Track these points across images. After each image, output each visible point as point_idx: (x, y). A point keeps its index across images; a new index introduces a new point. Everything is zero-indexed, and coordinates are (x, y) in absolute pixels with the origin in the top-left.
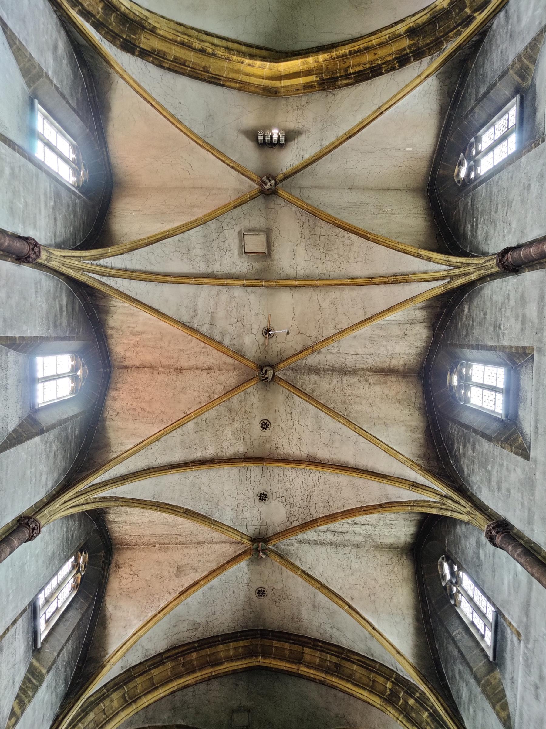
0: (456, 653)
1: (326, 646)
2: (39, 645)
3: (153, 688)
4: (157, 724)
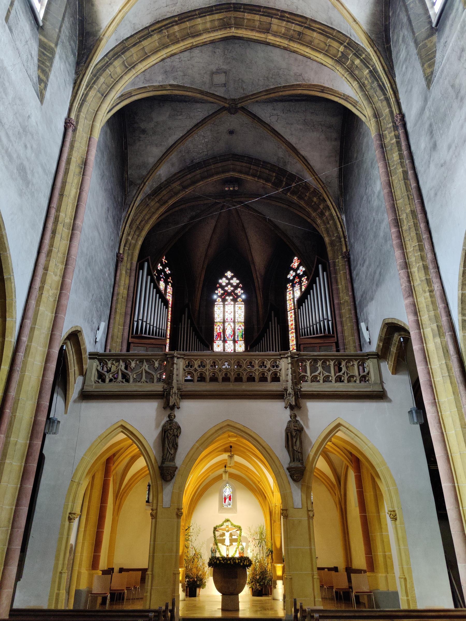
0: (405, 20)
2: (41, 24)
3: (146, 57)
4: (154, 84)
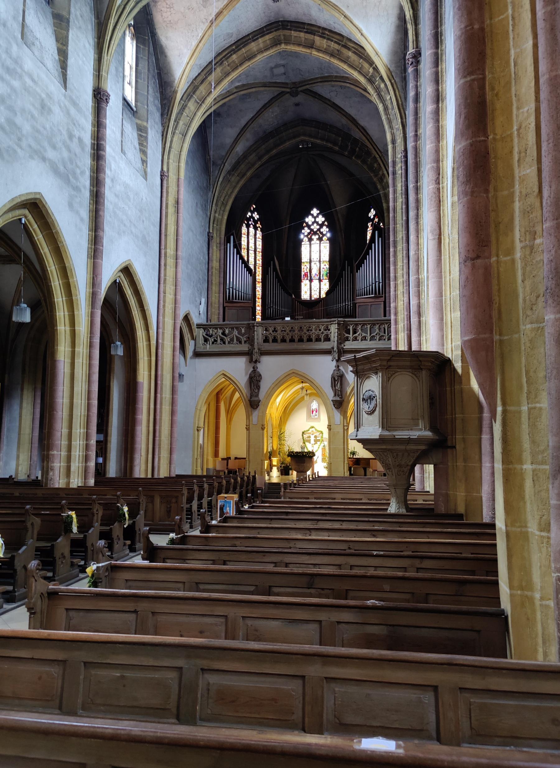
1: (331, 34)
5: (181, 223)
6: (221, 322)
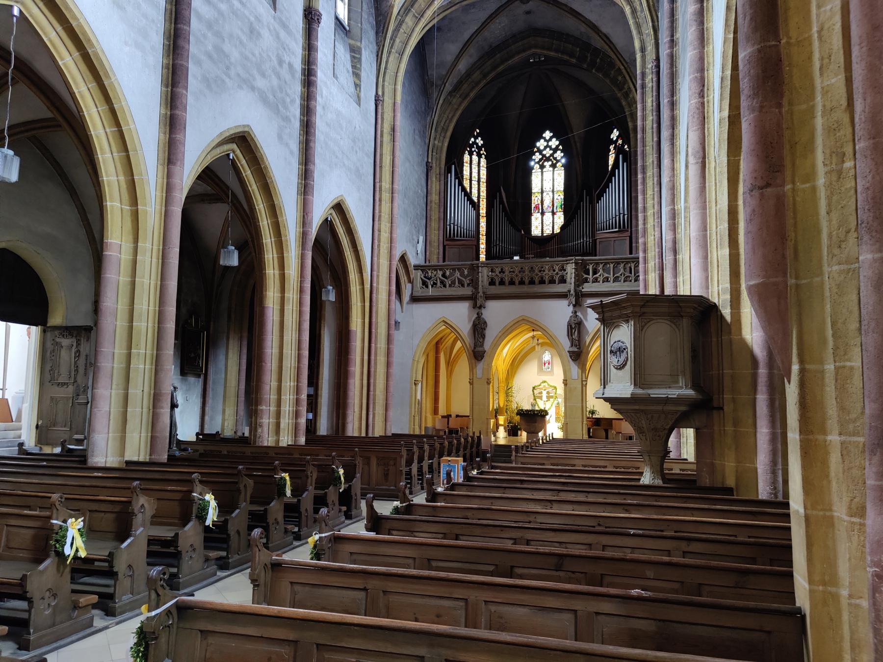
5: (397, 153)
6: (441, 263)
